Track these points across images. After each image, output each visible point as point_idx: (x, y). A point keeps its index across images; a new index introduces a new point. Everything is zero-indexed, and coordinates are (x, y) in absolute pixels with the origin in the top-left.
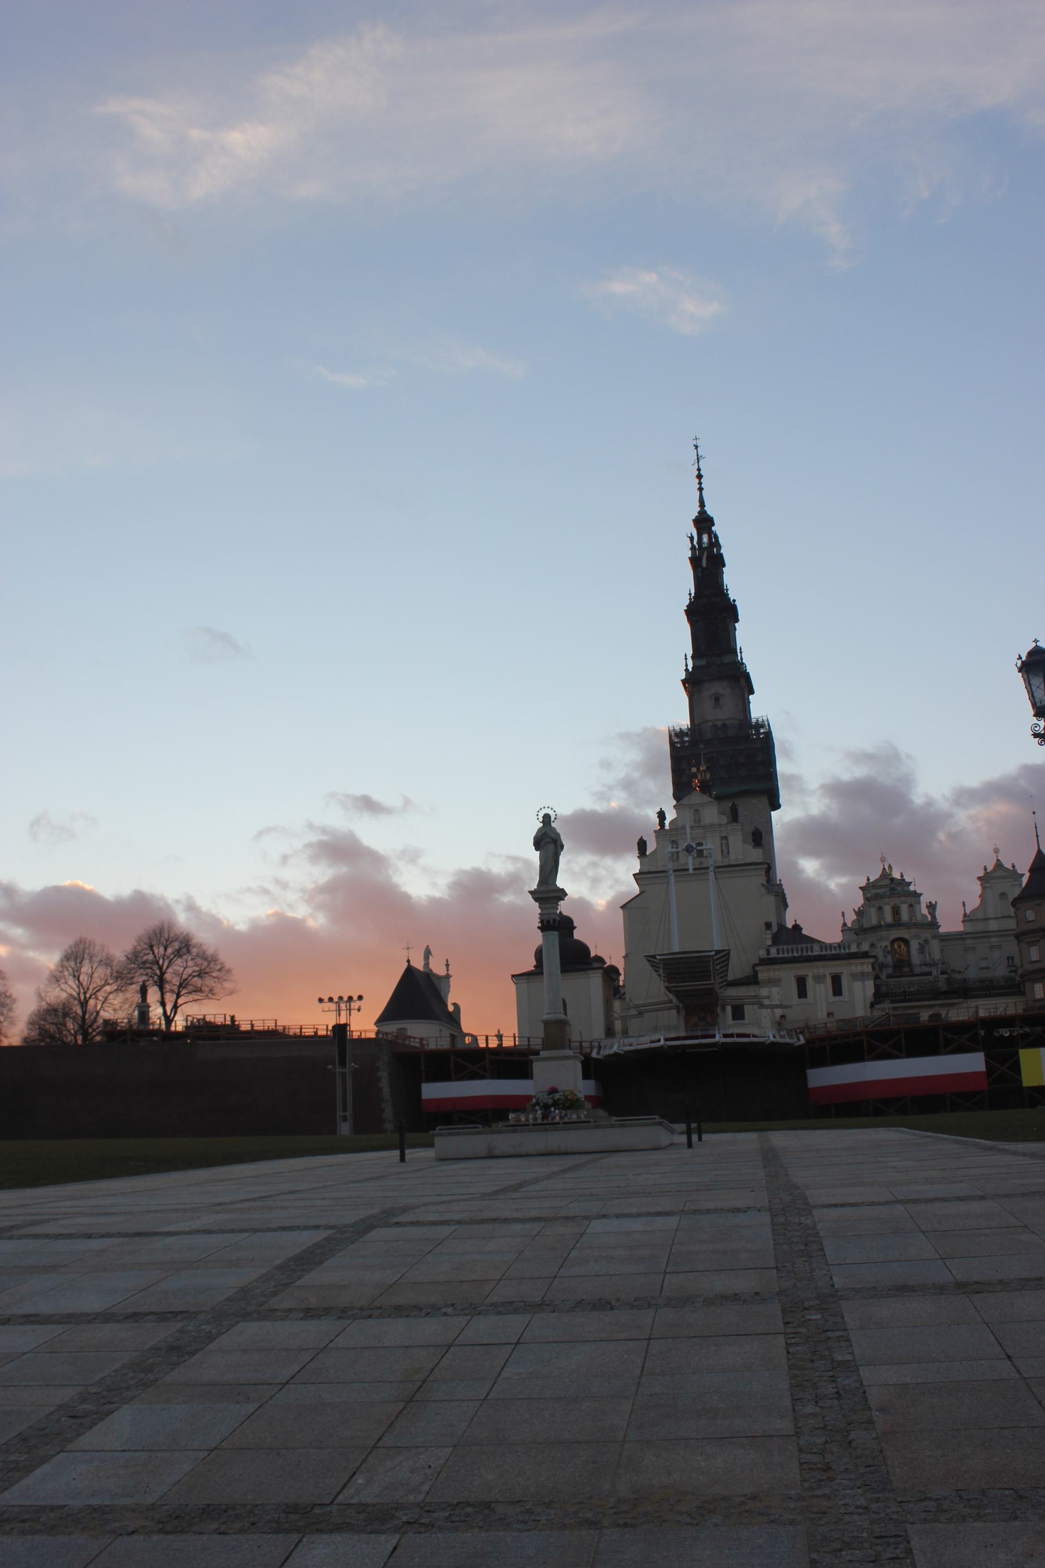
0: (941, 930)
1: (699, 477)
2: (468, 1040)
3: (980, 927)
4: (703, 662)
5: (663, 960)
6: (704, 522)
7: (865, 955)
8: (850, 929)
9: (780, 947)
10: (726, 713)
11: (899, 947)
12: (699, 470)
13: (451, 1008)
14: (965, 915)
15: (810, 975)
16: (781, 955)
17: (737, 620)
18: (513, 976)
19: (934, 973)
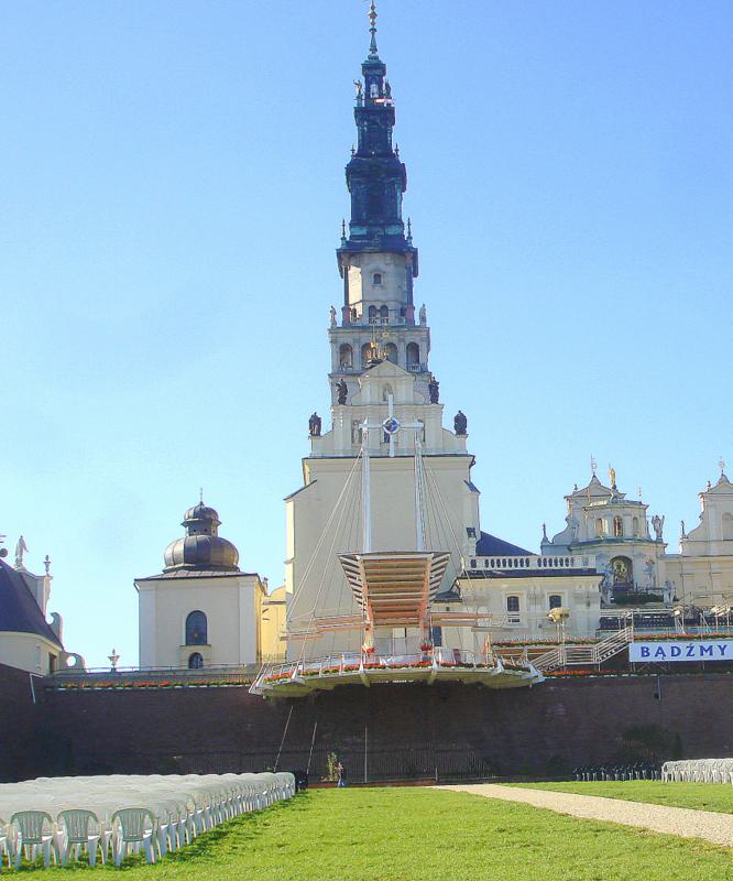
0: (668, 551)
1: (373, 16)
3: (701, 549)
4: (364, 231)
5: (364, 561)
6: (374, 71)
7: (592, 572)
8: (552, 546)
9: (489, 559)
11: (619, 567)
12: (373, 8)
14: (684, 537)
15: (525, 596)
16: (490, 568)
17: (404, 190)
19: (666, 597)
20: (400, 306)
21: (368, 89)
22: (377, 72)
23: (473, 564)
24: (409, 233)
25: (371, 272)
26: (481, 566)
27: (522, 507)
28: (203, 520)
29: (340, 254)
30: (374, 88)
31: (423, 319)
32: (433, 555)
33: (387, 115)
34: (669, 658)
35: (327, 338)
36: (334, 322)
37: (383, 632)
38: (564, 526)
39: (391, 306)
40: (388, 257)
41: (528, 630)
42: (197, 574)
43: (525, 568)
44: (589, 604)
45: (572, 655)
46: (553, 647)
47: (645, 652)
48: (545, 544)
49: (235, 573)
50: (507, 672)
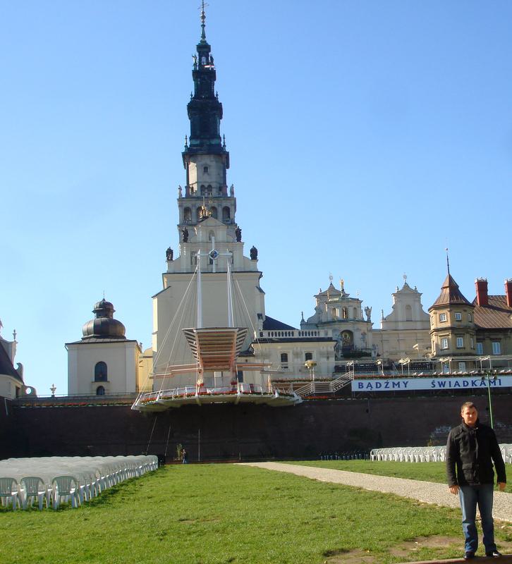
1: (203, 17)
2: (28, 391)
3: (393, 326)
4: (198, 142)
6: (204, 49)
7: (330, 340)
9: (271, 331)
10: (212, 179)
11: (346, 336)
12: (203, 13)
13: (16, 367)
14: (383, 319)
15: (291, 351)
16: (271, 337)
17: (221, 118)
18: (66, 344)
19: (373, 353)
20: (218, 185)
21: (200, 59)
22: (205, 50)
23: (261, 334)
24: (224, 143)
25: (202, 166)
26: (265, 335)
27: (290, 303)
28: (105, 309)
29: (184, 155)
30: (204, 59)
31: (232, 193)
32: (237, 330)
33: (211, 75)
34: (374, 389)
35: (176, 204)
36: (181, 195)
37: (208, 374)
38: (313, 313)
39: (214, 185)
40: (212, 157)
41: (293, 373)
42: (101, 340)
43: (291, 337)
44: (328, 358)
45: (317, 387)
46: (307, 382)
47: (361, 385)
48: (303, 323)
49: (123, 340)
50: (281, 397)
